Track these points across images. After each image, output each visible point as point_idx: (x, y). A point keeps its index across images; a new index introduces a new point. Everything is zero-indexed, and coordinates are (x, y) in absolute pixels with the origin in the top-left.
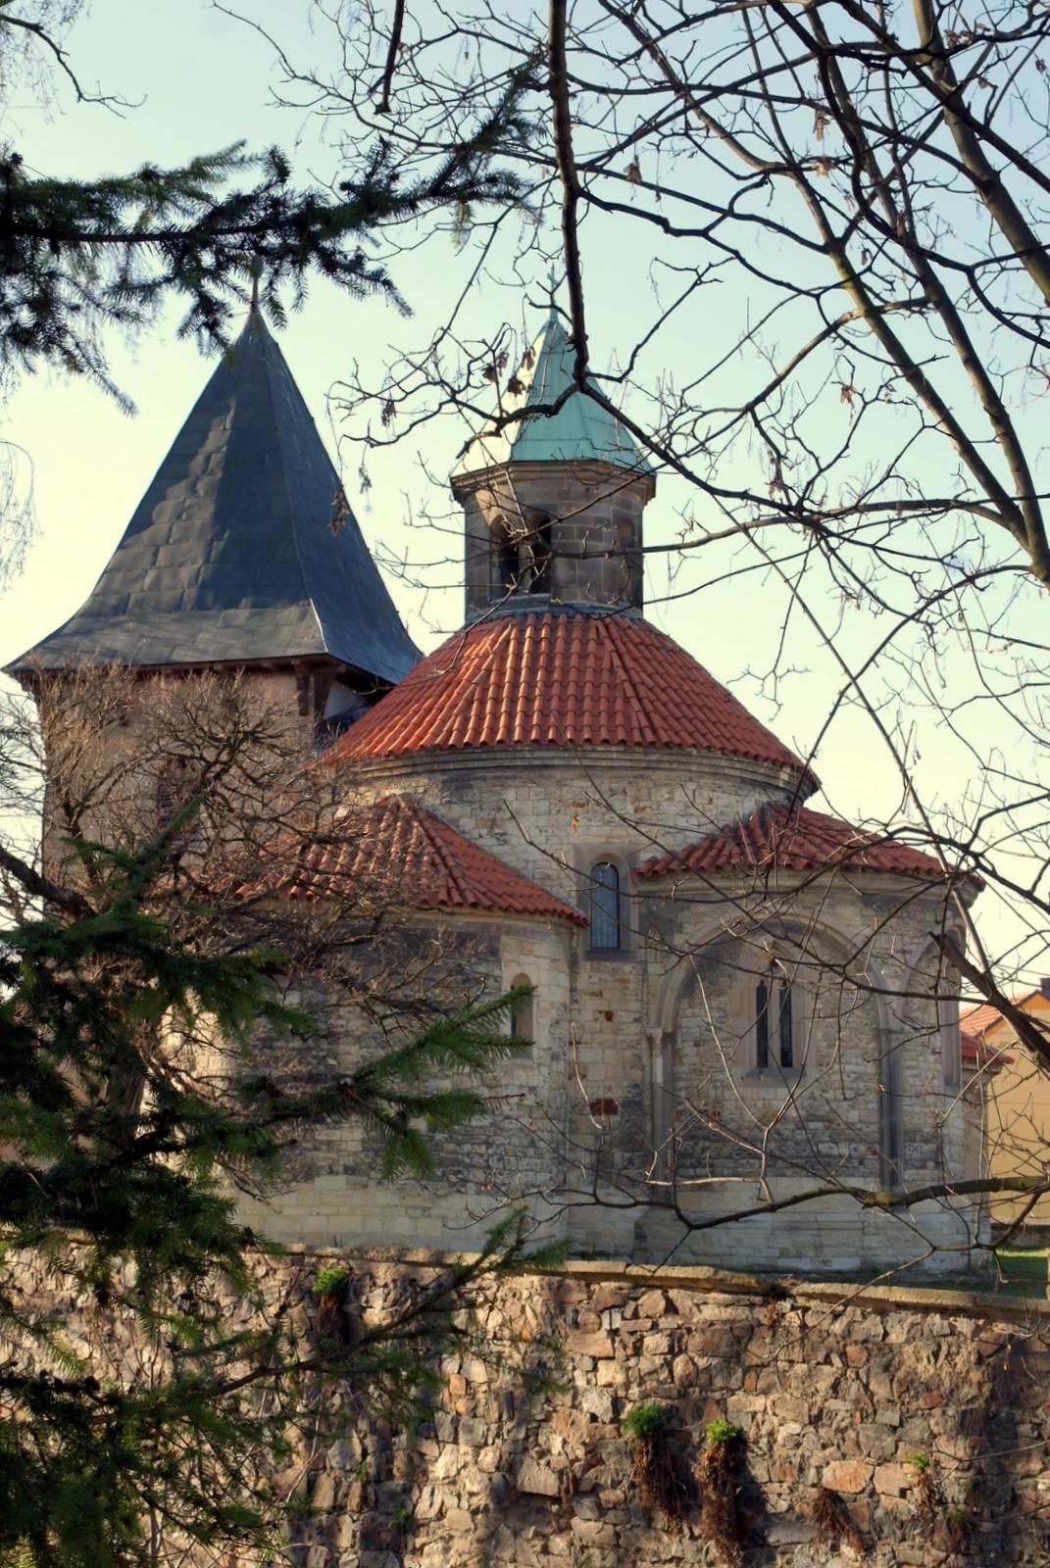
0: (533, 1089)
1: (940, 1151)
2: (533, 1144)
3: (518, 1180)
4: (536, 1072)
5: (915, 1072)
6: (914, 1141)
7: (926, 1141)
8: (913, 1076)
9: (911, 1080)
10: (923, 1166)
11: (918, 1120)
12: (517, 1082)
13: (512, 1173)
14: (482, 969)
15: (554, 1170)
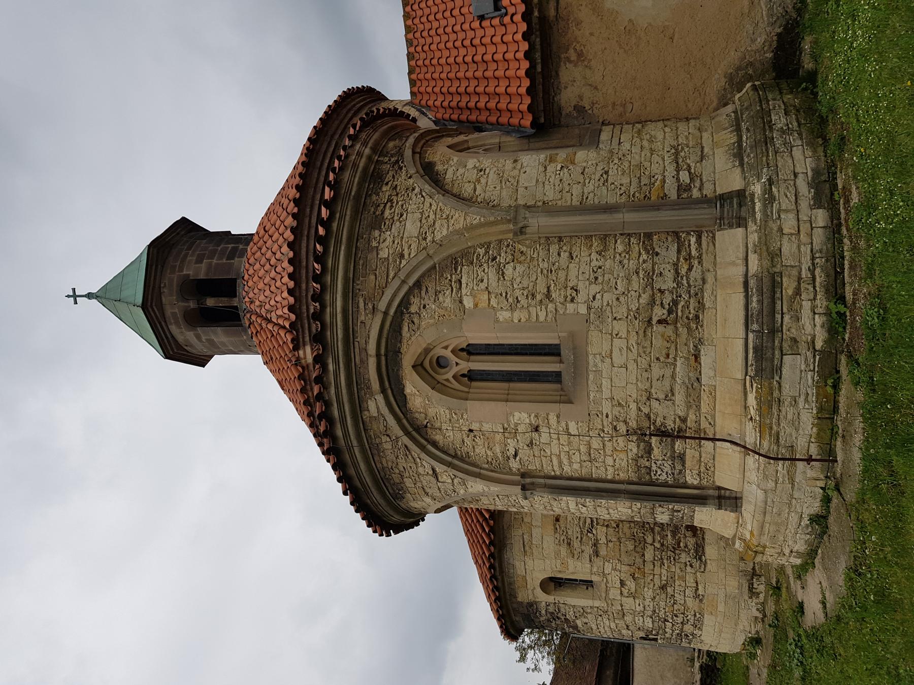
0: (622, 583)
1: (662, 433)
2: (663, 588)
3: (690, 602)
4: (609, 577)
5: (565, 461)
6: (650, 468)
7: (649, 451)
8: (571, 463)
9: (576, 466)
10: (682, 457)
11: (622, 460)
12: (619, 597)
13: (686, 608)
14: (543, 612)
15: (684, 557)
